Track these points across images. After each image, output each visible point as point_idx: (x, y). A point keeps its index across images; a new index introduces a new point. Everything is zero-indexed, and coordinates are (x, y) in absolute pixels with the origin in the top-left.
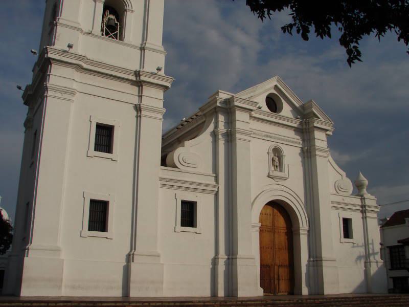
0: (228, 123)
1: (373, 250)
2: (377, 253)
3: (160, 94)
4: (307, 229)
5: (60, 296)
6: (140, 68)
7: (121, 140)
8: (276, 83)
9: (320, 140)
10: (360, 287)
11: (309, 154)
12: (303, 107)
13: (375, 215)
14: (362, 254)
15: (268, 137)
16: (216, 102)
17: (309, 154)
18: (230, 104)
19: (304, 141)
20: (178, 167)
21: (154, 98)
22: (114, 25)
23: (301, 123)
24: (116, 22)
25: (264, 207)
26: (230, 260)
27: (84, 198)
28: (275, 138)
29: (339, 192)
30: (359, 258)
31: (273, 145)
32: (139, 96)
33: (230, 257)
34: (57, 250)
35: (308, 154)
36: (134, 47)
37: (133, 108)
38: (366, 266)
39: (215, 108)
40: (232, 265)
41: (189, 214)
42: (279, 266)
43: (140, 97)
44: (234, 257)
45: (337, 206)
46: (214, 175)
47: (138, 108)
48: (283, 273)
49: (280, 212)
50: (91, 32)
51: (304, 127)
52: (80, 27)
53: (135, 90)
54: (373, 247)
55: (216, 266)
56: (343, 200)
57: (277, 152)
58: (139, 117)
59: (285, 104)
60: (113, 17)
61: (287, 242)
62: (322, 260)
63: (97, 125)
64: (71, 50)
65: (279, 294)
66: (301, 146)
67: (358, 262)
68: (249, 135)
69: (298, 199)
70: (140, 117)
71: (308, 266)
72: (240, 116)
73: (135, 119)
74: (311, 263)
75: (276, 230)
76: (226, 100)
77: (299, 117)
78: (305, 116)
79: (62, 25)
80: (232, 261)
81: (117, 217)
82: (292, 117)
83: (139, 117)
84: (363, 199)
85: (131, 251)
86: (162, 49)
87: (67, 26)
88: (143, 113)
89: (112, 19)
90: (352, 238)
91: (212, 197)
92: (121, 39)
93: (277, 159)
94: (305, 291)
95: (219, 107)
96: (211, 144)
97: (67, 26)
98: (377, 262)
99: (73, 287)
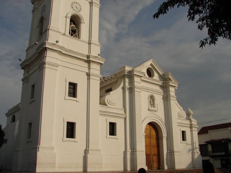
0: (130, 83)
1: (196, 146)
2: (197, 148)
3: (98, 67)
4: (166, 136)
5: (55, 172)
6: (89, 54)
7: (81, 91)
8: (151, 62)
9: (172, 91)
10: (190, 165)
11: (167, 99)
12: (164, 74)
13: (196, 129)
14: (190, 149)
15: (147, 90)
16: (125, 72)
17: (167, 99)
18: (131, 73)
19: (164, 92)
20: (107, 105)
21: (95, 70)
22: (75, 30)
23: (163, 83)
24: (76, 29)
25: (147, 125)
26: (133, 152)
27: (64, 121)
28: (151, 90)
29: (180, 118)
30: (189, 150)
31: (150, 94)
32: (88, 68)
33: (133, 151)
34: (53, 148)
35: (166, 98)
36: (85, 42)
37: (85, 74)
38: (192, 155)
39: (124, 75)
40: (134, 155)
41: (112, 129)
42: (153, 155)
43: (89, 69)
44: (134, 150)
45: (180, 125)
46: (124, 109)
47: (88, 75)
48: (155, 158)
49: (153, 128)
50: (65, 33)
51: (165, 85)
52: (59, 31)
53: (86, 65)
54: (196, 145)
55: (126, 155)
56: (182, 122)
57: (152, 98)
58: (89, 79)
60: (74, 26)
61: (156, 143)
62: (174, 152)
63: (69, 83)
64: (57, 44)
65: (154, 169)
66: (163, 95)
67: (189, 152)
68: (140, 89)
69: (162, 122)
70: (90, 79)
71: (167, 155)
72: (136, 79)
73: (87, 80)
74: (168, 153)
75: (152, 137)
76: (129, 71)
77: (162, 80)
78: (165, 79)
79: (51, 30)
80: (134, 153)
81: (79, 130)
82: (159, 80)
83: (89, 79)
84: (191, 121)
85: (87, 148)
86: (98, 44)
87: (54, 31)
88: (91, 77)
89: (73, 27)
90: (186, 141)
91: (123, 120)
92: (79, 38)
93: (152, 101)
94: (166, 167)
95: (126, 74)
96: (122, 93)
97: (54, 31)
98: (198, 153)
99: (60, 167)
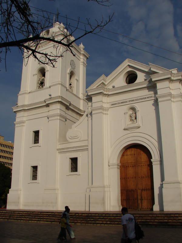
28: (129, 101)
42: (142, 190)
59: (138, 73)
66: (154, 98)
